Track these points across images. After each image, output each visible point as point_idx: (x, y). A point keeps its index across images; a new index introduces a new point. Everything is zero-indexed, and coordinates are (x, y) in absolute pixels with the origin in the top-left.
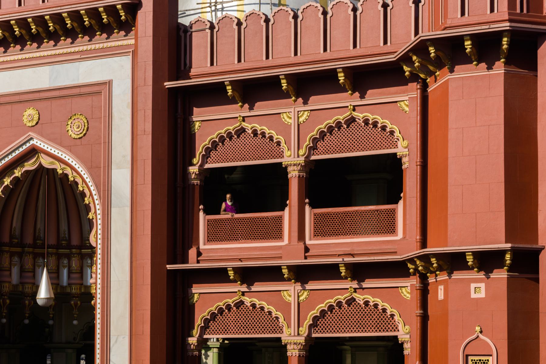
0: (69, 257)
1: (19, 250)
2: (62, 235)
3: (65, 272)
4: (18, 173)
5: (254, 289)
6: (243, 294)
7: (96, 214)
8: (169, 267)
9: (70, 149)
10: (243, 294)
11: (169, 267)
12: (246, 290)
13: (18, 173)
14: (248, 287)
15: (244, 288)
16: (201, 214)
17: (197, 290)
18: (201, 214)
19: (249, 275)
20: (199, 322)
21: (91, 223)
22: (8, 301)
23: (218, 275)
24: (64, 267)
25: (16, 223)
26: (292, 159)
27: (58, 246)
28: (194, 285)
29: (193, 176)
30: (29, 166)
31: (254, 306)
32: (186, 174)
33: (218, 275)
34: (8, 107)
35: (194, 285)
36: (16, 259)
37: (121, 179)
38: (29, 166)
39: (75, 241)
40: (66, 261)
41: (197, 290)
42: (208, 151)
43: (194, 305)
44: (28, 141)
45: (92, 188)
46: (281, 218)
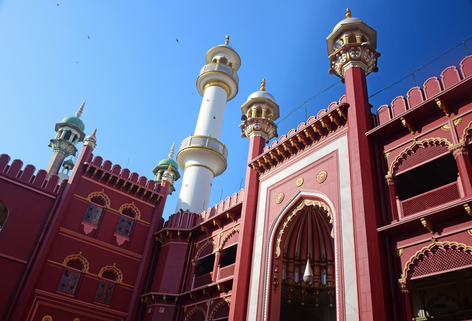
0: (326, 268)
1: (299, 263)
2: (322, 255)
3: (325, 276)
4: (294, 213)
5: (443, 235)
6: (437, 240)
7: (334, 221)
8: (379, 229)
9: (318, 189)
10: (437, 240)
11: (379, 229)
12: (439, 236)
13: (294, 213)
14: (440, 234)
15: (437, 236)
16: (398, 201)
17: (401, 246)
18: (398, 201)
19: (438, 223)
20: (405, 267)
21: (331, 226)
22: (292, 290)
23: (413, 229)
24: (324, 274)
25: (297, 250)
26: (455, 146)
27: (320, 262)
28: (397, 243)
29: (388, 180)
30: (300, 208)
31: (446, 247)
32: (384, 180)
33: (413, 229)
34: (290, 182)
35: (397, 243)
36: (297, 269)
37: (345, 193)
38: (300, 208)
39: (329, 258)
40: (325, 271)
41: (401, 246)
42: (397, 165)
43: (399, 258)
44: (298, 194)
45: (331, 206)
46: (456, 186)
